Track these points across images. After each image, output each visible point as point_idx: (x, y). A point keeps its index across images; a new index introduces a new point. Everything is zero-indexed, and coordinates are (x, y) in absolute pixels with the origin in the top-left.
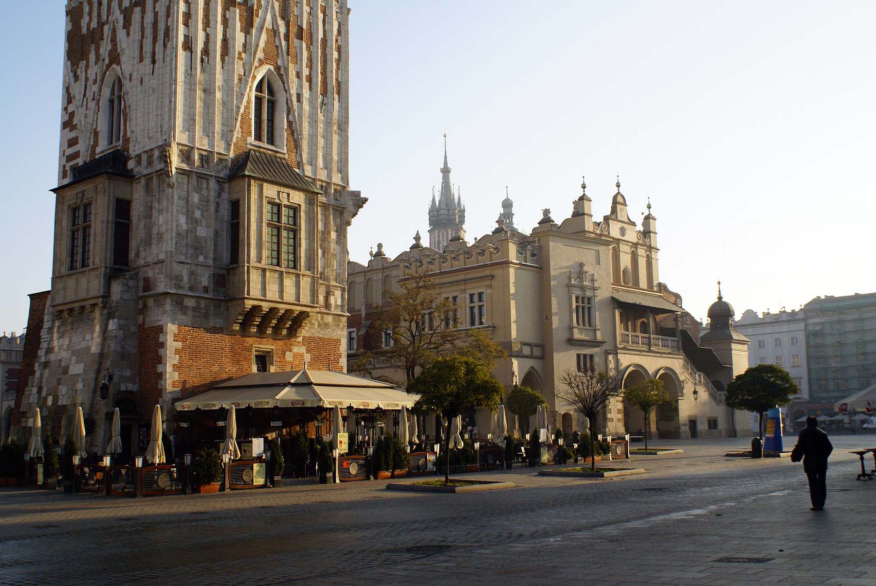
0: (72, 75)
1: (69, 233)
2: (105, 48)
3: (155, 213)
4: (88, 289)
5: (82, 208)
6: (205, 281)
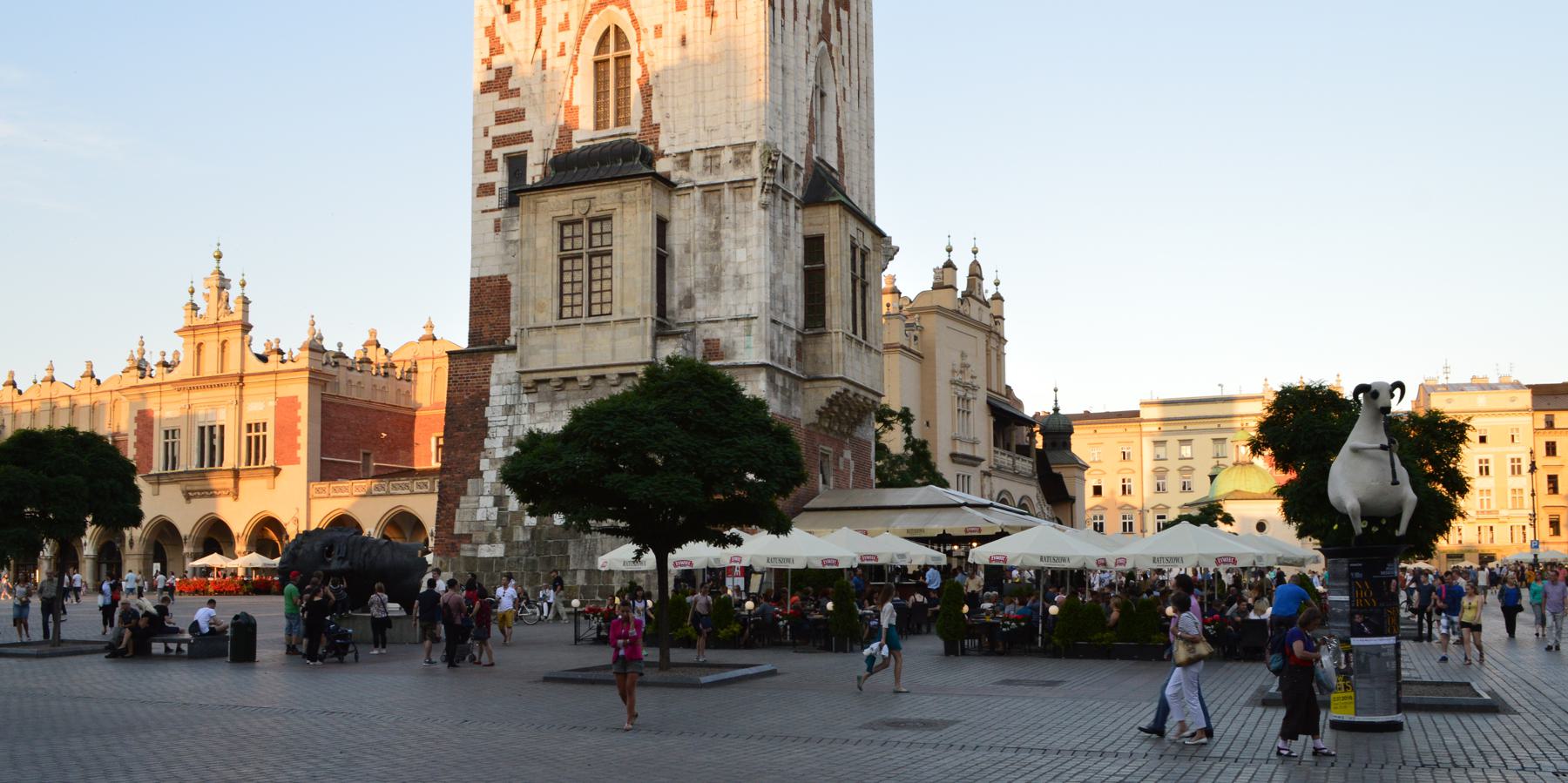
0: (501, 9)
1: (556, 261)
3: (728, 245)
4: (613, 351)
6: (790, 352)
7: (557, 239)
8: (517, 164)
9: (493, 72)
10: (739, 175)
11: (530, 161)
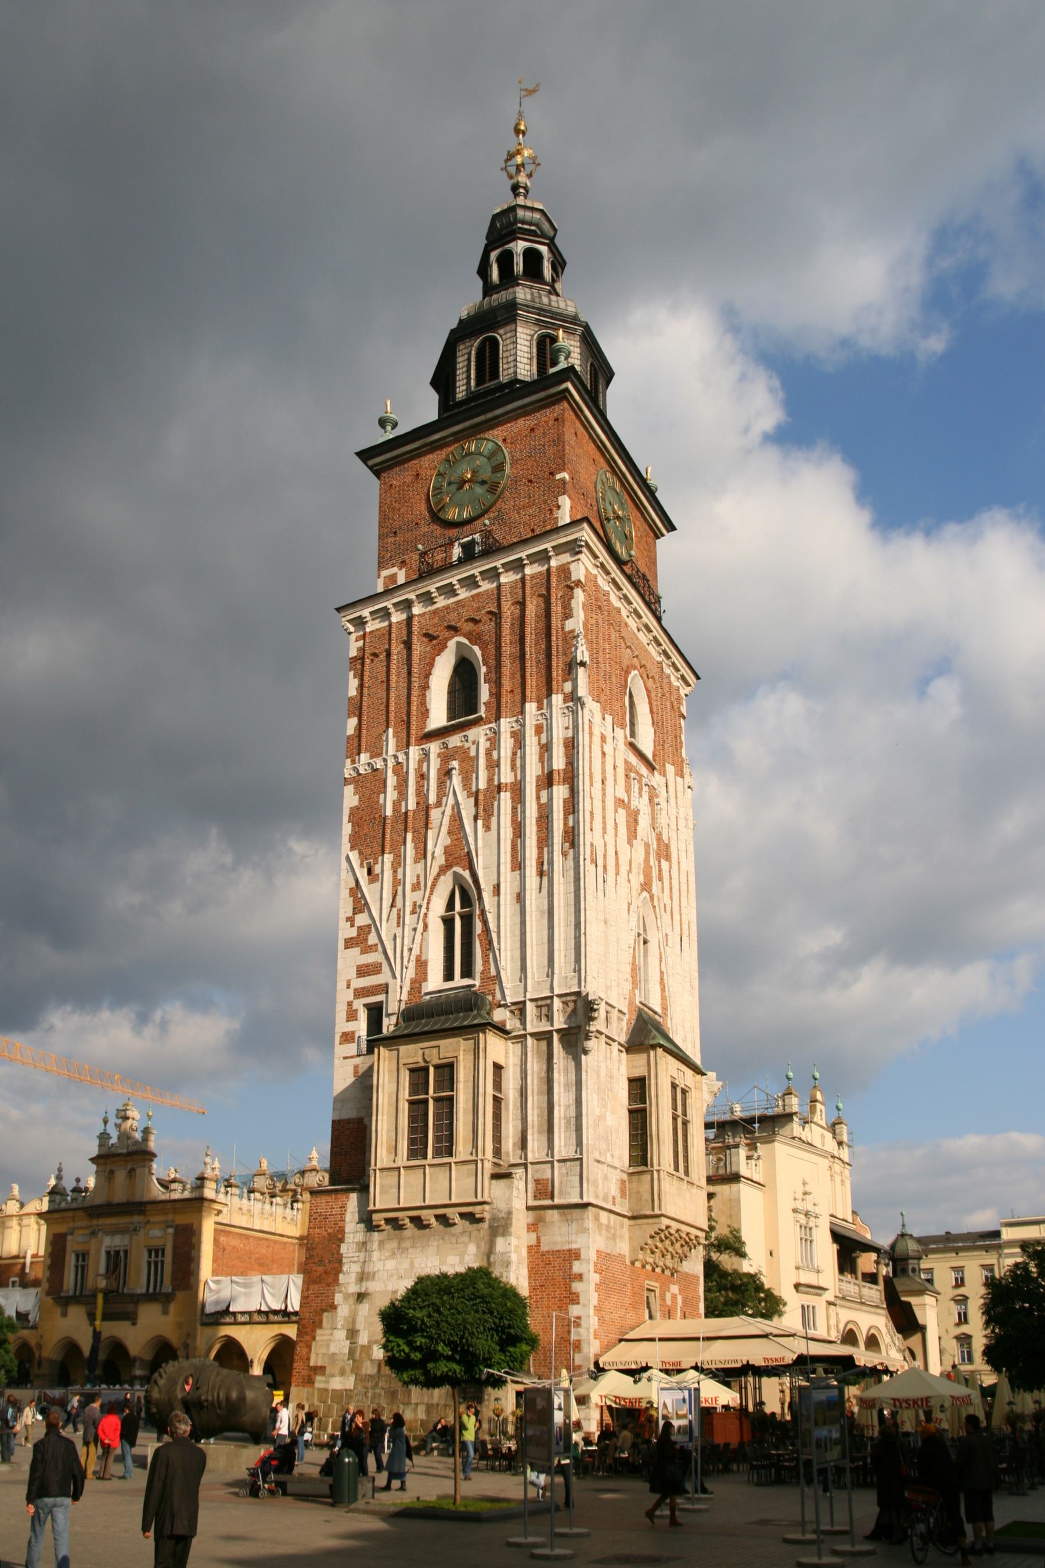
0: (362, 874)
9: (355, 929)
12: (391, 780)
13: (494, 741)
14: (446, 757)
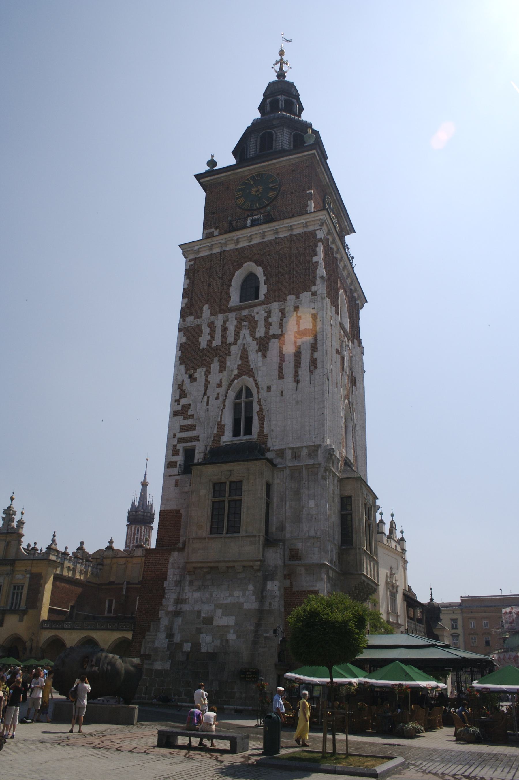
1: (210, 503)
2: (233, 363)
5: (228, 483)
7: (212, 491)
8: (189, 453)
9: (180, 406)
10: (311, 462)
11: (196, 451)
12: (206, 330)
13: (269, 313)
14: (240, 320)
